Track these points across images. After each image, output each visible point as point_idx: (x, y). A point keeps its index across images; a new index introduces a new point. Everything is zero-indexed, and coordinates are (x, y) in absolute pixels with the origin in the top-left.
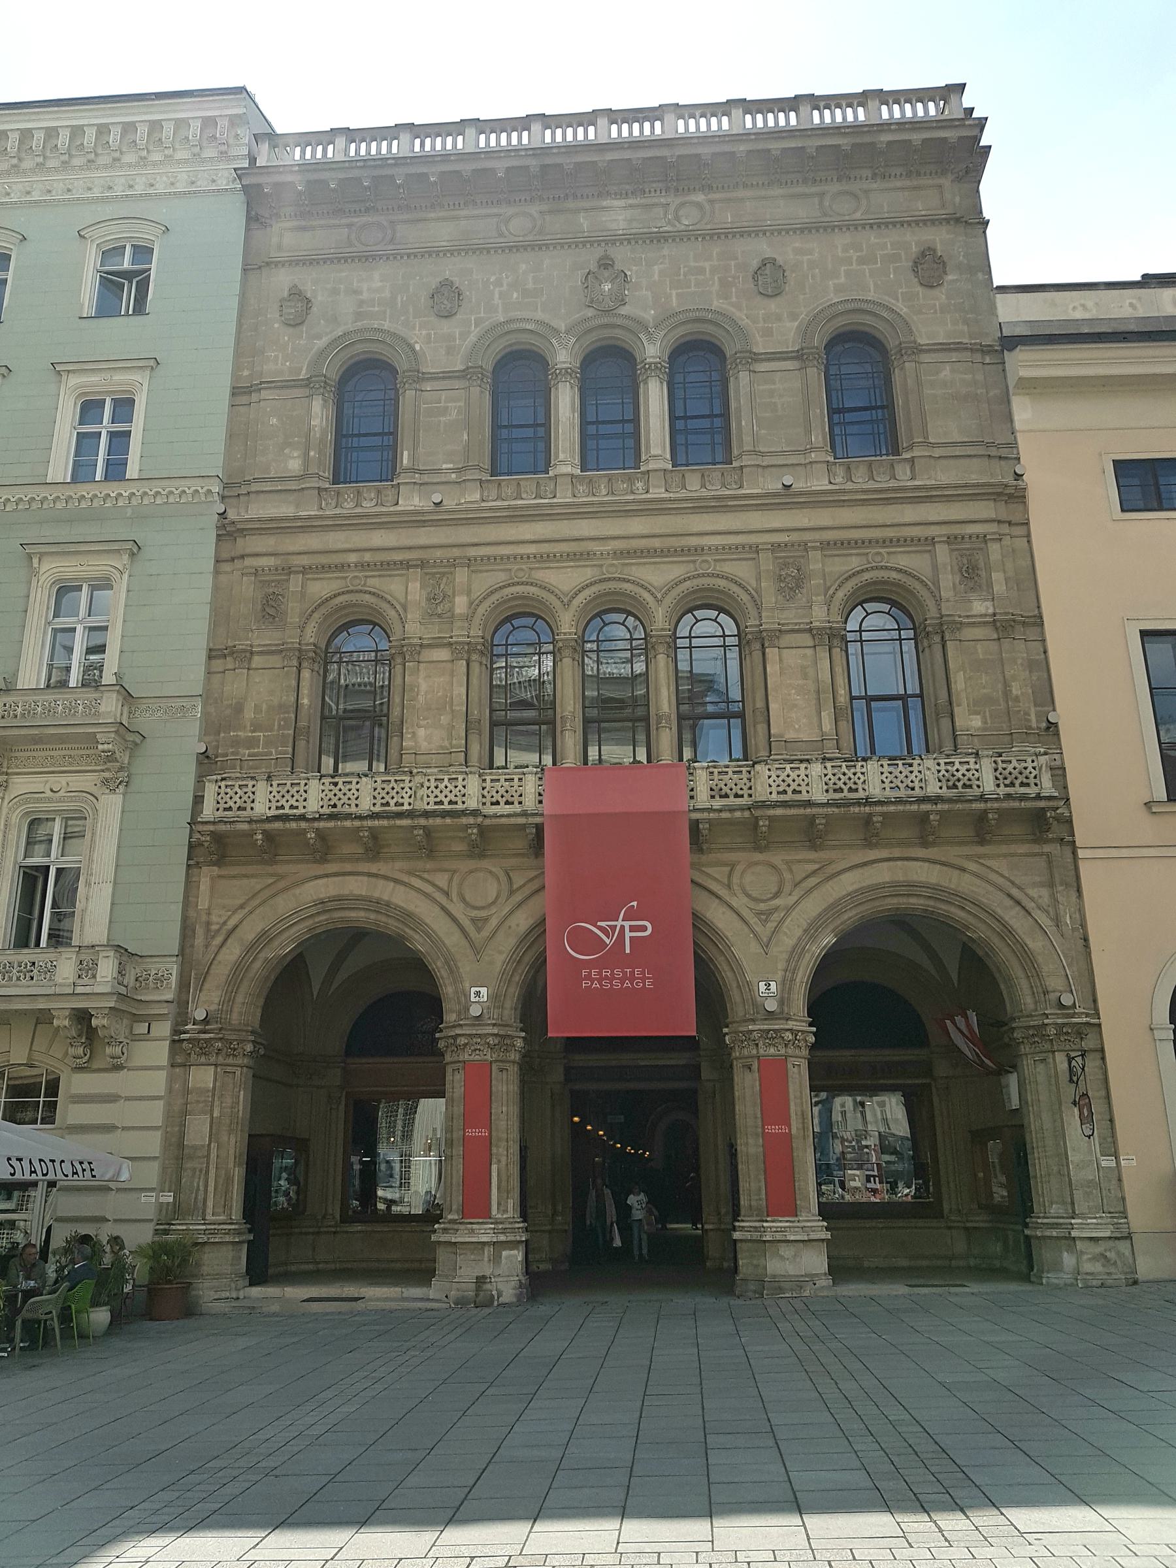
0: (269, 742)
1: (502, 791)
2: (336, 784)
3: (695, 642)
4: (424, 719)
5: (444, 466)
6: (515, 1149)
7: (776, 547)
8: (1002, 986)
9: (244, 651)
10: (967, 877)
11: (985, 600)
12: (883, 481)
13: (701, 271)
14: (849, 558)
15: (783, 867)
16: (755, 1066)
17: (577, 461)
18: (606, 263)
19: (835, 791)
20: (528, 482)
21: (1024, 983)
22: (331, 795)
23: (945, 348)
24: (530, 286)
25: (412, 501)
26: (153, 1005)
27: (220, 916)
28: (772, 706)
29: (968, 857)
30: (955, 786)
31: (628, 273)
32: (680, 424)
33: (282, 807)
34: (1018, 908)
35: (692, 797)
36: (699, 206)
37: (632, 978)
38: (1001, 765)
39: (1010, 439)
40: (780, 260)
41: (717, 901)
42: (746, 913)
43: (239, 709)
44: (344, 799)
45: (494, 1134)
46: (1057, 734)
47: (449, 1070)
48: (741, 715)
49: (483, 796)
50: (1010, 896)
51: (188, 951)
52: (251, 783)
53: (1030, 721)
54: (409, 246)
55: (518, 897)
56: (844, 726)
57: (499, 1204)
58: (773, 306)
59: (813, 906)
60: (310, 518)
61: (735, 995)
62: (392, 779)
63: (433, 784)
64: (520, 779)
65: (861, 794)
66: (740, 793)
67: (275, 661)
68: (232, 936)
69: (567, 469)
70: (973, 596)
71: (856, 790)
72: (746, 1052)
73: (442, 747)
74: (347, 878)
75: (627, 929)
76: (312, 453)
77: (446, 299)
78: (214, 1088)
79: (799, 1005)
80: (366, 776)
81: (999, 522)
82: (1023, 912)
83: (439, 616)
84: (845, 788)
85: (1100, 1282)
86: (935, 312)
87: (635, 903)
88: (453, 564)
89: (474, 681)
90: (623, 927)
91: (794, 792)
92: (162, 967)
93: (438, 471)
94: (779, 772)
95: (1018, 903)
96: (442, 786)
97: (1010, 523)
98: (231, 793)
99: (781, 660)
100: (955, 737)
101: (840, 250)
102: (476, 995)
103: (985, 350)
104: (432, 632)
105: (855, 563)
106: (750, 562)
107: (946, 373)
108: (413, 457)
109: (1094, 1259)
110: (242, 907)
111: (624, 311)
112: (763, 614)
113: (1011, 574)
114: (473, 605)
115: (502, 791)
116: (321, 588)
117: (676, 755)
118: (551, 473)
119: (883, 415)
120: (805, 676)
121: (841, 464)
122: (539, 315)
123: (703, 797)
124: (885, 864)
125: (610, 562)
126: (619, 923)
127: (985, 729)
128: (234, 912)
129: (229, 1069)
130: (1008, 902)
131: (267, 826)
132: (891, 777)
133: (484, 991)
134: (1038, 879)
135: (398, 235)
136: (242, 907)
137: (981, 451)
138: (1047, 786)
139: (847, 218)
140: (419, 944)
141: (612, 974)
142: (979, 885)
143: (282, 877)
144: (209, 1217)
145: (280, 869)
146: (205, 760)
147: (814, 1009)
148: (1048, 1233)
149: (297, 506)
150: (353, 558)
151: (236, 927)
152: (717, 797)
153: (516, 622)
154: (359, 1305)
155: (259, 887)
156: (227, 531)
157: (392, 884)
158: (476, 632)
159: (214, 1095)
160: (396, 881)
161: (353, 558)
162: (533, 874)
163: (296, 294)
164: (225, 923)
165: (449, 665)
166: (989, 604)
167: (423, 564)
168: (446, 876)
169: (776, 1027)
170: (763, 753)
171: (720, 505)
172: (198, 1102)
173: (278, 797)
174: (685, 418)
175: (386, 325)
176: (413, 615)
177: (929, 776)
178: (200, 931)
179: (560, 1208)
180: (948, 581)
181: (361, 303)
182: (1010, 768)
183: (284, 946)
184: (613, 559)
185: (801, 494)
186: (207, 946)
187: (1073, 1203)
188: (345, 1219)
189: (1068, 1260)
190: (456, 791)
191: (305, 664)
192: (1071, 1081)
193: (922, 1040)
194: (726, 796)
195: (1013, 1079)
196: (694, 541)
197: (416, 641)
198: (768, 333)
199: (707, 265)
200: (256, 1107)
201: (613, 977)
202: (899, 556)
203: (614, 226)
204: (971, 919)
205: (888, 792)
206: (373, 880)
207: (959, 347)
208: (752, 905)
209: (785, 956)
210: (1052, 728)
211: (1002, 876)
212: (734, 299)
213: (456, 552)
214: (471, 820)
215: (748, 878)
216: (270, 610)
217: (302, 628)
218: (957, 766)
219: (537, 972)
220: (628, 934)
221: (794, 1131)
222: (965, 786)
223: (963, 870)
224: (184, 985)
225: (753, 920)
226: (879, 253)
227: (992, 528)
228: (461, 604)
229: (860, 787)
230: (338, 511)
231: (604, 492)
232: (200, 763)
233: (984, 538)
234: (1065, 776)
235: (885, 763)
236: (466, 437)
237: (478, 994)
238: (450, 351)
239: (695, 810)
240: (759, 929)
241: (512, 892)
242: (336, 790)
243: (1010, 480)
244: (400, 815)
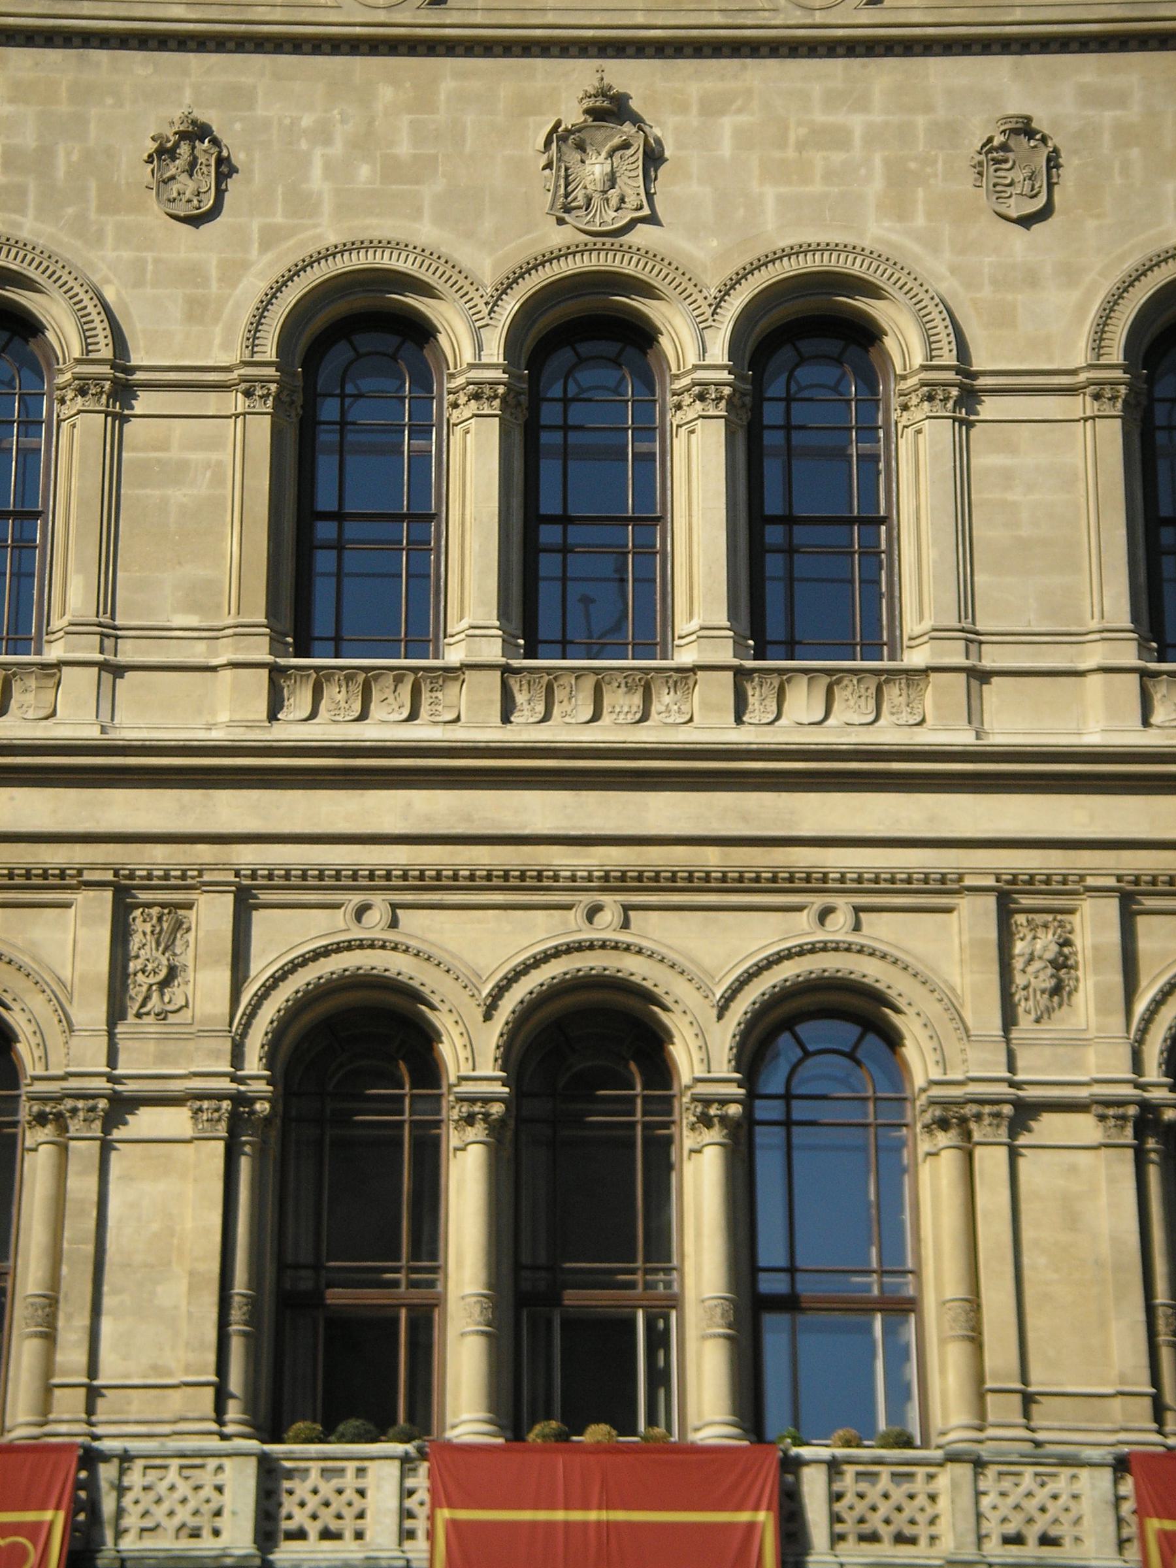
13: (837, 138)
24: (404, 149)
64: (361, 1472)
111: (642, 236)
174: (789, 520)
198: (1003, 318)
199: (857, 122)
212: (920, 221)
238: (198, 311)
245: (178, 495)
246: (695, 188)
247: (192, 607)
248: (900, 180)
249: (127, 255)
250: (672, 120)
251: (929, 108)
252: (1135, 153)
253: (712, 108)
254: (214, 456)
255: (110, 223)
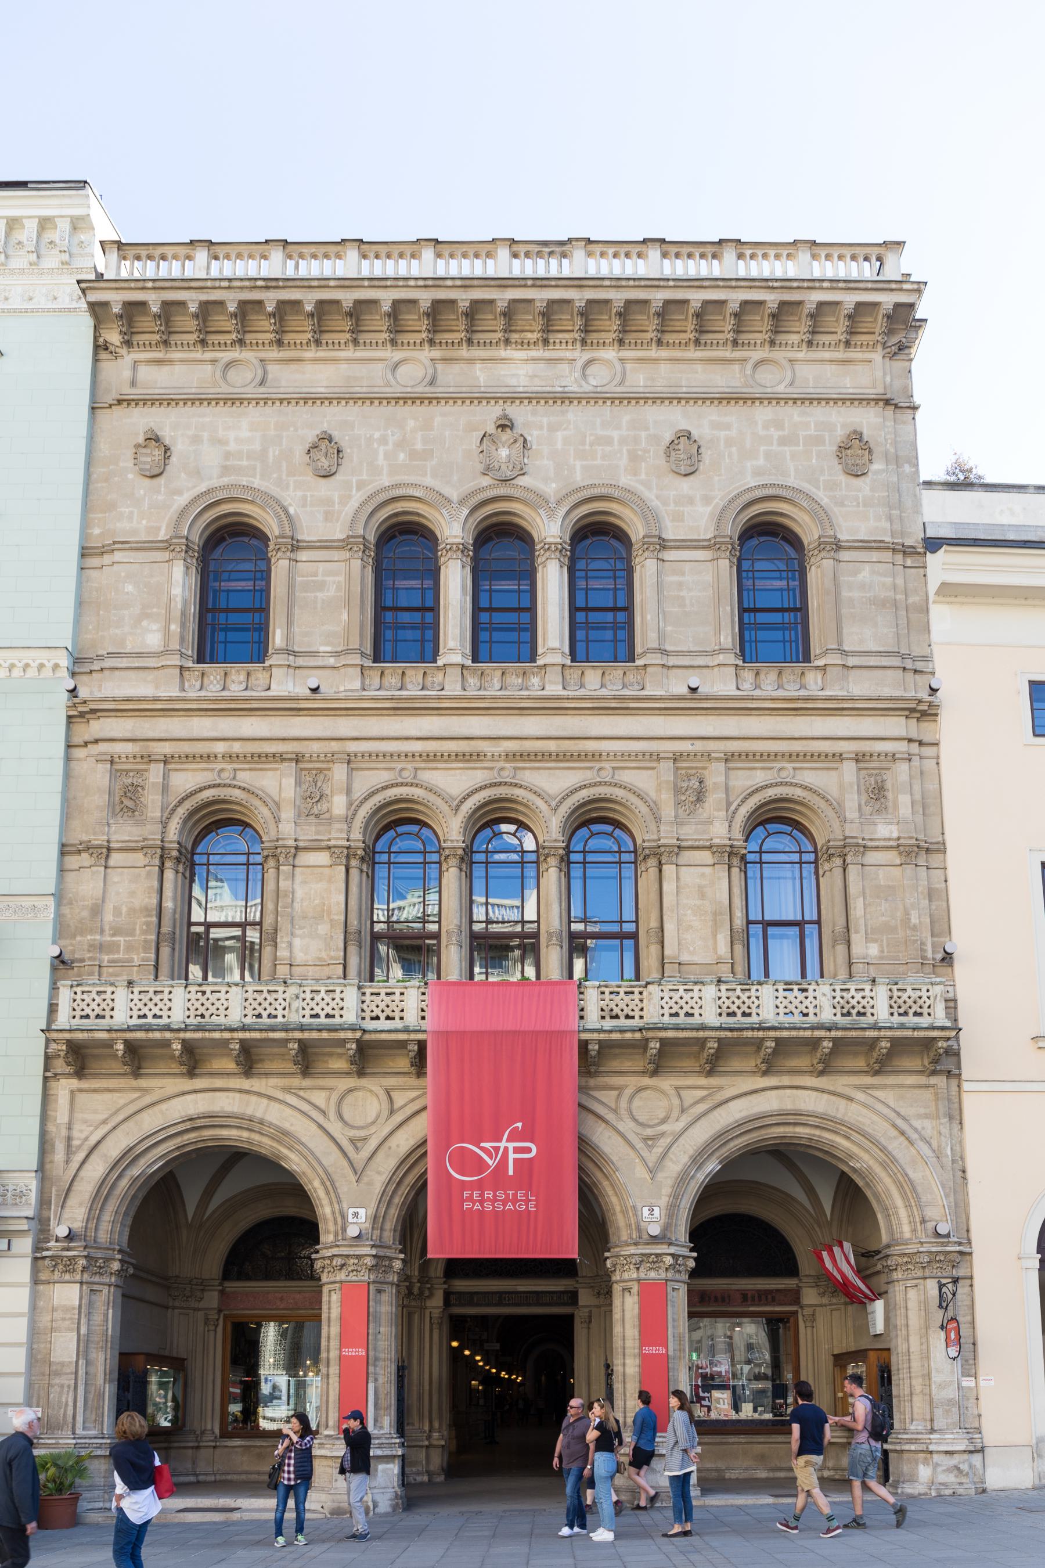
0: (129, 948)
1: (382, 1005)
2: (204, 993)
3: (590, 858)
4: (301, 928)
5: (322, 649)
6: (393, 1368)
7: (677, 757)
8: (879, 1216)
9: (100, 847)
10: (854, 1106)
11: (890, 823)
12: (791, 690)
13: (608, 441)
14: (753, 772)
15: (673, 1092)
16: (635, 1289)
17: (468, 650)
18: (505, 425)
19: (729, 1015)
20: (414, 673)
21: (903, 1213)
22: (198, 1005)
23: (866, 546)
24: (419, 446)
25: (285, 684)
26: (11, 1222)
27: (81, 1131)
28: (666, 926)
29: (858, 1087)
30: (849, 1014)
31: (529, 438)
32: (580, 616)
33: (145, 1016)
34: (902, 1139)
35: (582, 1018)
36: (607, 362)
37: (515, 1201)
38: (896, 994)
39: (926, 652)
40: (695, 434)
41: (604, 1125)
42: (631, 1137)
43: (96, 910)
44: (213, 1009)
45: (371, 1353)
46: (951, 965)
47: (325, 1290)
48: (634, 936)
49: (363, 1011)
50: (894, 1126)
51: (48, 1166)
52: (109, 989)
53: (925, 951)
54: (282, 390)
55: (398, 1118)
56: (739, 948)
57: (376, 1421)
58: (685, 486)
59: (701, 1134)
60: (170, 700)
61: (620, 1220)
62: (265, 989)
63: (308, 996)
65: (754, 1019)
66: (631, 1014)
67: (139, 858)
68: (96, 1152)
69: (457, 659)
70: (877, 818)
71: (750, 1015)
72: (626, 1276)
73: (320, 959)
74: (218, 1094)
75: (510, 1150)
76: (173, 627)
77: (327, 454)
78: (80, 1306)
79: (682, 1232)
80: (237, 985)
81: (910, 740)
82: (906, 1142)
83: (317, 816)
84: (739, 1013)
85: (951, 1492)
86: (858, 505)
87: (519, 1125)
88: (331, 758)
89: (354, 889)
90: (506, 1149)
91: (687, 1014)
92: (21, 1182)
93: (313, 654)
94: (672, 994)
95: (902, 1133)
96: (318, 998)
97: (921, 743)
98: (88, 1000)
99: (678, 878)
100: (850, 964)
101: (760, 426)
102: (351, 1214)
103: (907, 551)
104: (308, 833)
105: (760, 777)
106: (650, 772)
107: (865, 574)
108: (288, 637)
109: (948, 1470)
110: (104, 1122)
111: (522, 481)
112: (662, 828)
113: (918, 797)
114: (354, 807)
115: (382, 1005)
116: (185, 780)
117: (566, 974)
118: (440, 663)
119: (796, 618)
120: (702, 896)
121: (750, 669)
122: (429, 481)
123: (593, 1019)
124: (774, 1092)
125: (502, 764)
126: (503, 1144)
127: (882, 958)
128: (96, 1128)
129: (95, 1287)
130: (894, 1133)
131: (129, 1036)
132: (786, 1002)
133: (362, 1212)
134: (922, 1111)
135: (270, 376)
136: (104, 1122)
137: (896, 661)
138: (940, 1017)
139: (769, 390)
140: (294, 1162)
141: (495, 1196)
142: (861, 1118)
143: (145, 1091)
144: (79, 1431)
145: (143, 1083)
146: (61, 963)
147: (698, 1235)
148: (906, 1447)
149: (157, 688)
150: (220, 748)
151: (99, 1142)
152: (608, 1018)
153: (401, 829)
154: (236, 1516)
155: (122, 1102)
156: (80, 713)
157: (265, 1101)
158: (357, 835)
159: (80, 1313)
160: (270, 1098)
161: (220, 748)
162: (414, 1094)
163: (153, 438)
164: (86, 1139)
165: (327, 871)
166: (894, 828)
167: (298, 759)
168: (323, 1094)
169: (659, 1252)
170: (655, 975)
171: (620, 707)
172: (64, 1319)
173: (140, 1005)
175: (257, 482)
176: (287, 814)
177: (823, 1003)
178: (60, 1147)
179: (436, 1425)
180: (852, 803)
181: (227, 455)
182: (905, 996)
183: (149, 1164)
184: (506, 761)
185: (707, 698)
186: (67, 1162)
187: (932, 1420)
188: (225, 1435)
189: (924, 1472)
190: (333, 1004)
191: (168, 864)
192: (940, 1306)
193: (791, 1269)
194: (617, 1017)
195: (879, 1305)
196: (591, 746)
197: (291, 843)
198: (678, 517)
199: (615, 434)
200: (126, 1325)
201: (495, 1200)
202: (806, 773)
203: (513, 382)
204: (855, 1149)
205: (782, 1018)
206: (245, 1096)
207: (879, 546)
208: (639, 1129)
209: (670, 1182)
210: (948, 958)
211: (889, 1107)
213: (335, 746)
214: (349, 1035)
215: (637, 1103)
216: (127, 800)
217: (165, 825)
218: (853, 992)
219: (417, 1194)
220: (512, 1156)
221: (671, 1353)
222: (859, 1014)
223: (850, 1099)
224: (44, 1202)
225: (640, 1145)
226: (802, 434)
227: (903, 746)
228: (339, 805)
229: (754, 1011)
230: (203, 693)
231: (497, 686)
232: (54, 969)
233: (894, 758)
234: (956, 1008)
235: (781, 987)
236: (345, 616)
237: (356, 1215)
238: (328, 516)
239: (585, 1030)
240: (645, 1153)
241: (392, 1112)
242: (203, 999)
243: (924, 695)
244: (273, 1029)
245: (319, 595)
246: (545, 462)
247: (327, 644)
248: (634, 458)
249: (299, 493)
250: (535, 433)
251: (647, 429)
252: (734, 449)
253: (553, 428)
254: (337, 579)
255: (292, 479)
